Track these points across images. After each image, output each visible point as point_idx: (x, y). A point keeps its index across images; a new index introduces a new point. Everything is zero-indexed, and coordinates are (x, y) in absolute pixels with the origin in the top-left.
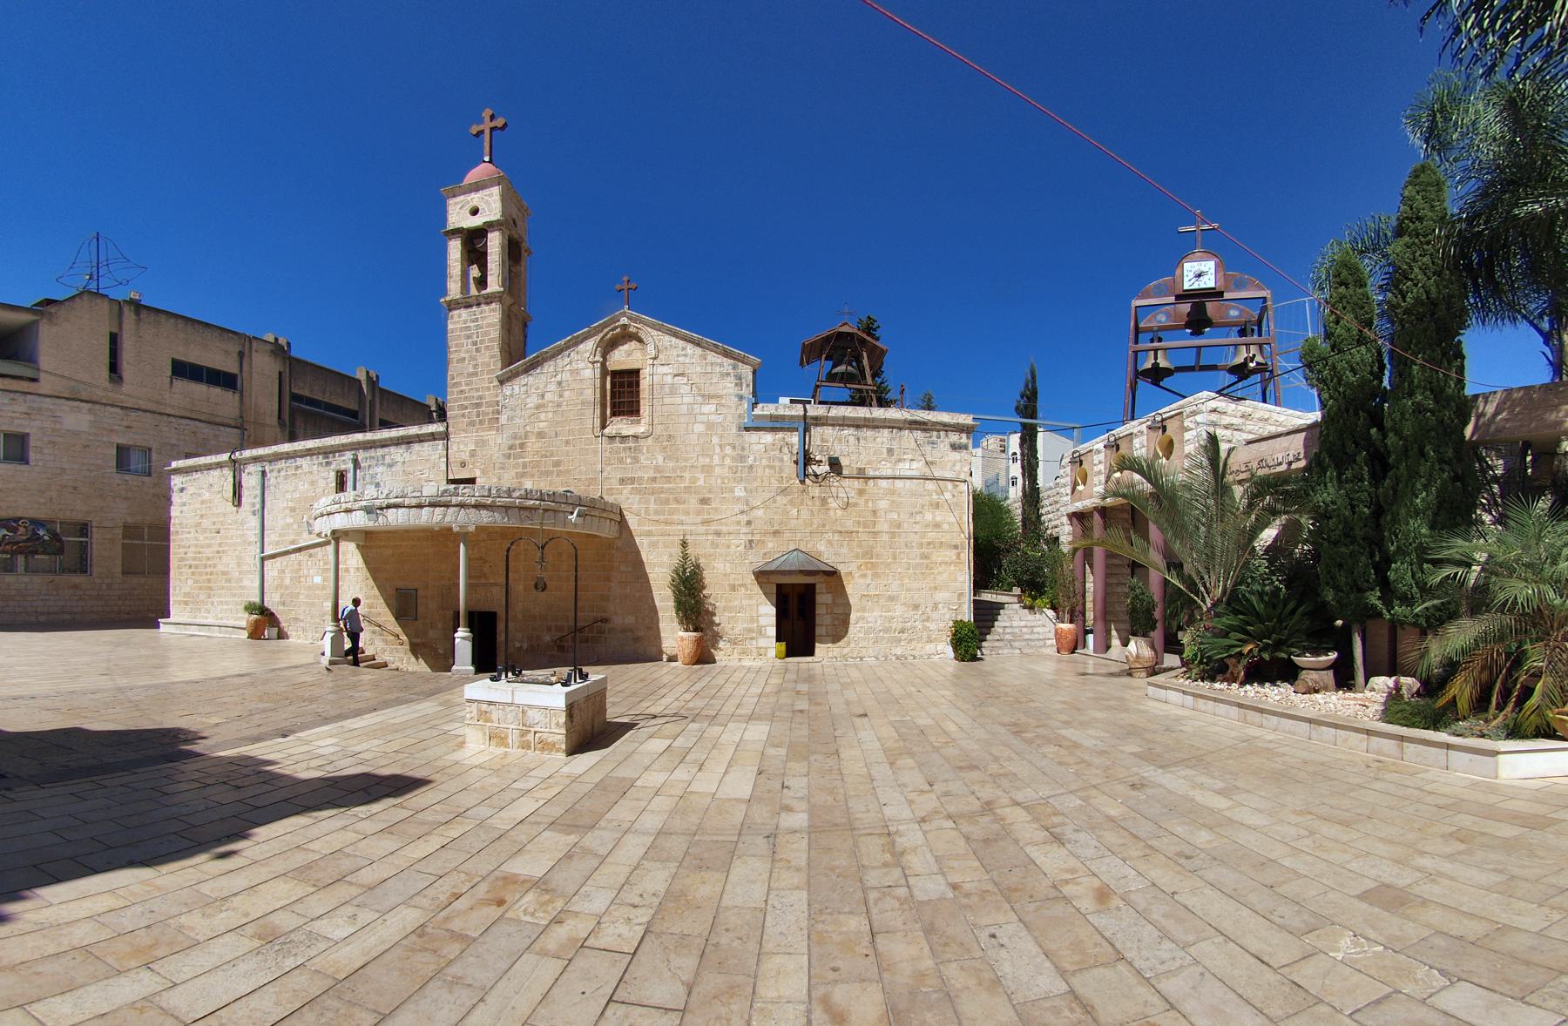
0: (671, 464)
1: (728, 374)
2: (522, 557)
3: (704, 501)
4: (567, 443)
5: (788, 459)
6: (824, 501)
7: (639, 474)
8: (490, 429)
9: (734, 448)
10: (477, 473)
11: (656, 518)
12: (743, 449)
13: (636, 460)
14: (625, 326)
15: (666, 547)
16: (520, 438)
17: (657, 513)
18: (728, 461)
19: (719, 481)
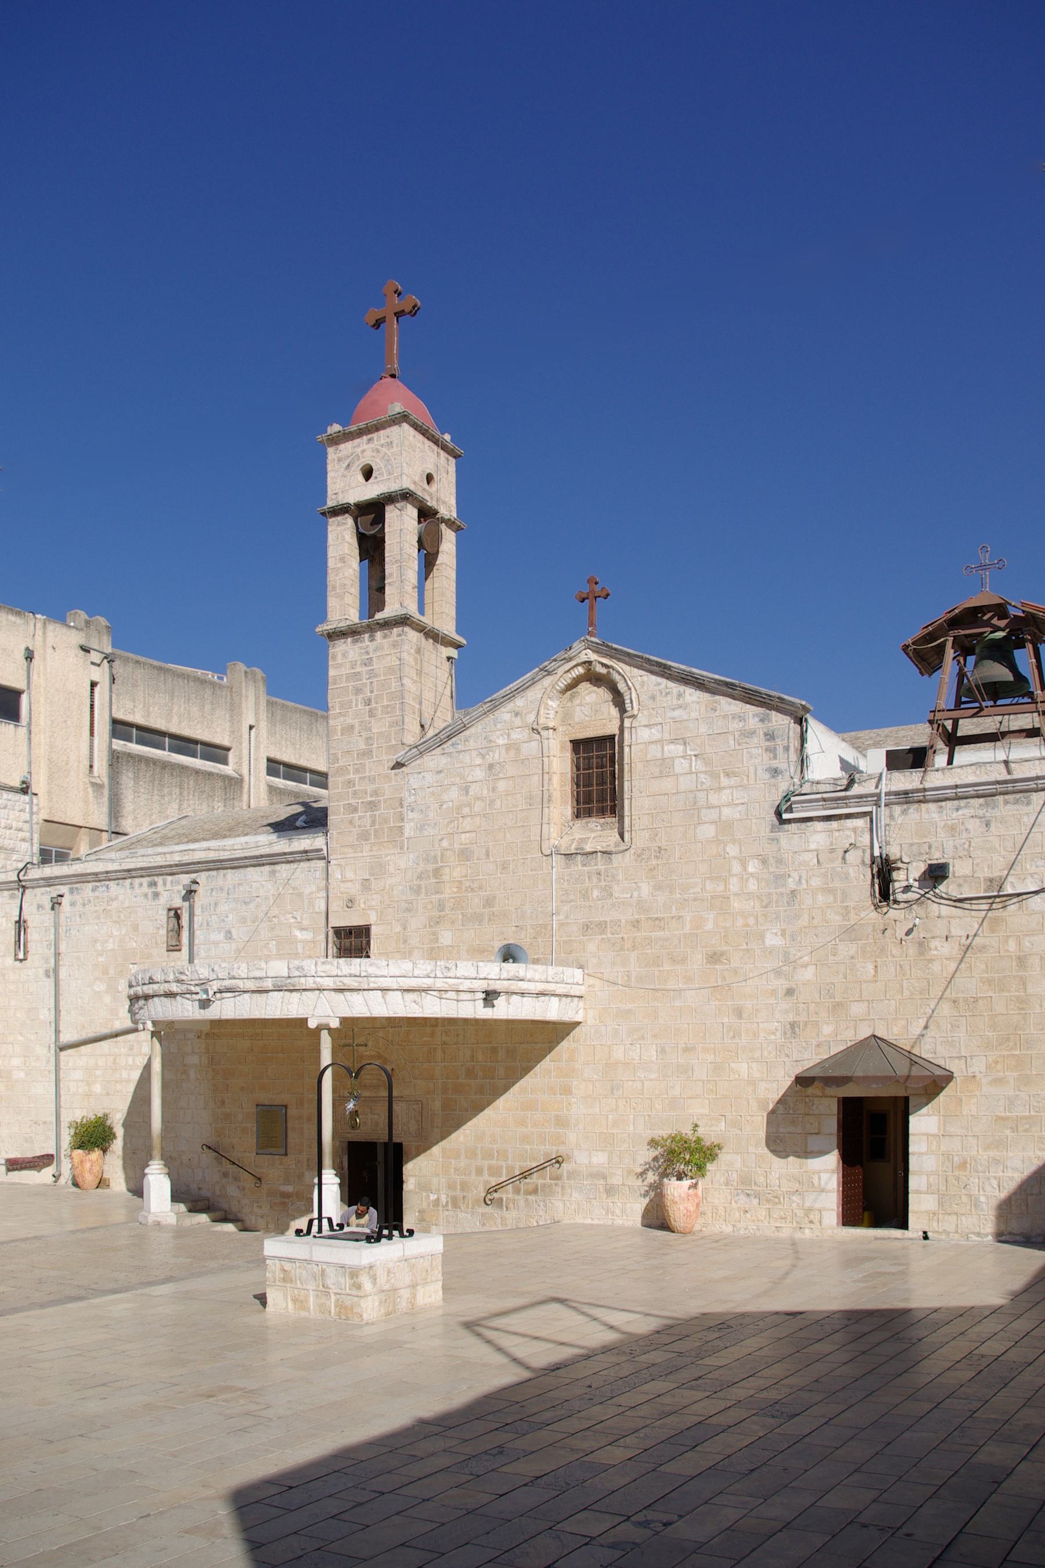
1: (752, 733)
2: (439, 1055)
3: (714, 958)
9: (764, 862)
12: (780, 861)
13: (608, 892)
18: (752, 886)
19: (740, 922)
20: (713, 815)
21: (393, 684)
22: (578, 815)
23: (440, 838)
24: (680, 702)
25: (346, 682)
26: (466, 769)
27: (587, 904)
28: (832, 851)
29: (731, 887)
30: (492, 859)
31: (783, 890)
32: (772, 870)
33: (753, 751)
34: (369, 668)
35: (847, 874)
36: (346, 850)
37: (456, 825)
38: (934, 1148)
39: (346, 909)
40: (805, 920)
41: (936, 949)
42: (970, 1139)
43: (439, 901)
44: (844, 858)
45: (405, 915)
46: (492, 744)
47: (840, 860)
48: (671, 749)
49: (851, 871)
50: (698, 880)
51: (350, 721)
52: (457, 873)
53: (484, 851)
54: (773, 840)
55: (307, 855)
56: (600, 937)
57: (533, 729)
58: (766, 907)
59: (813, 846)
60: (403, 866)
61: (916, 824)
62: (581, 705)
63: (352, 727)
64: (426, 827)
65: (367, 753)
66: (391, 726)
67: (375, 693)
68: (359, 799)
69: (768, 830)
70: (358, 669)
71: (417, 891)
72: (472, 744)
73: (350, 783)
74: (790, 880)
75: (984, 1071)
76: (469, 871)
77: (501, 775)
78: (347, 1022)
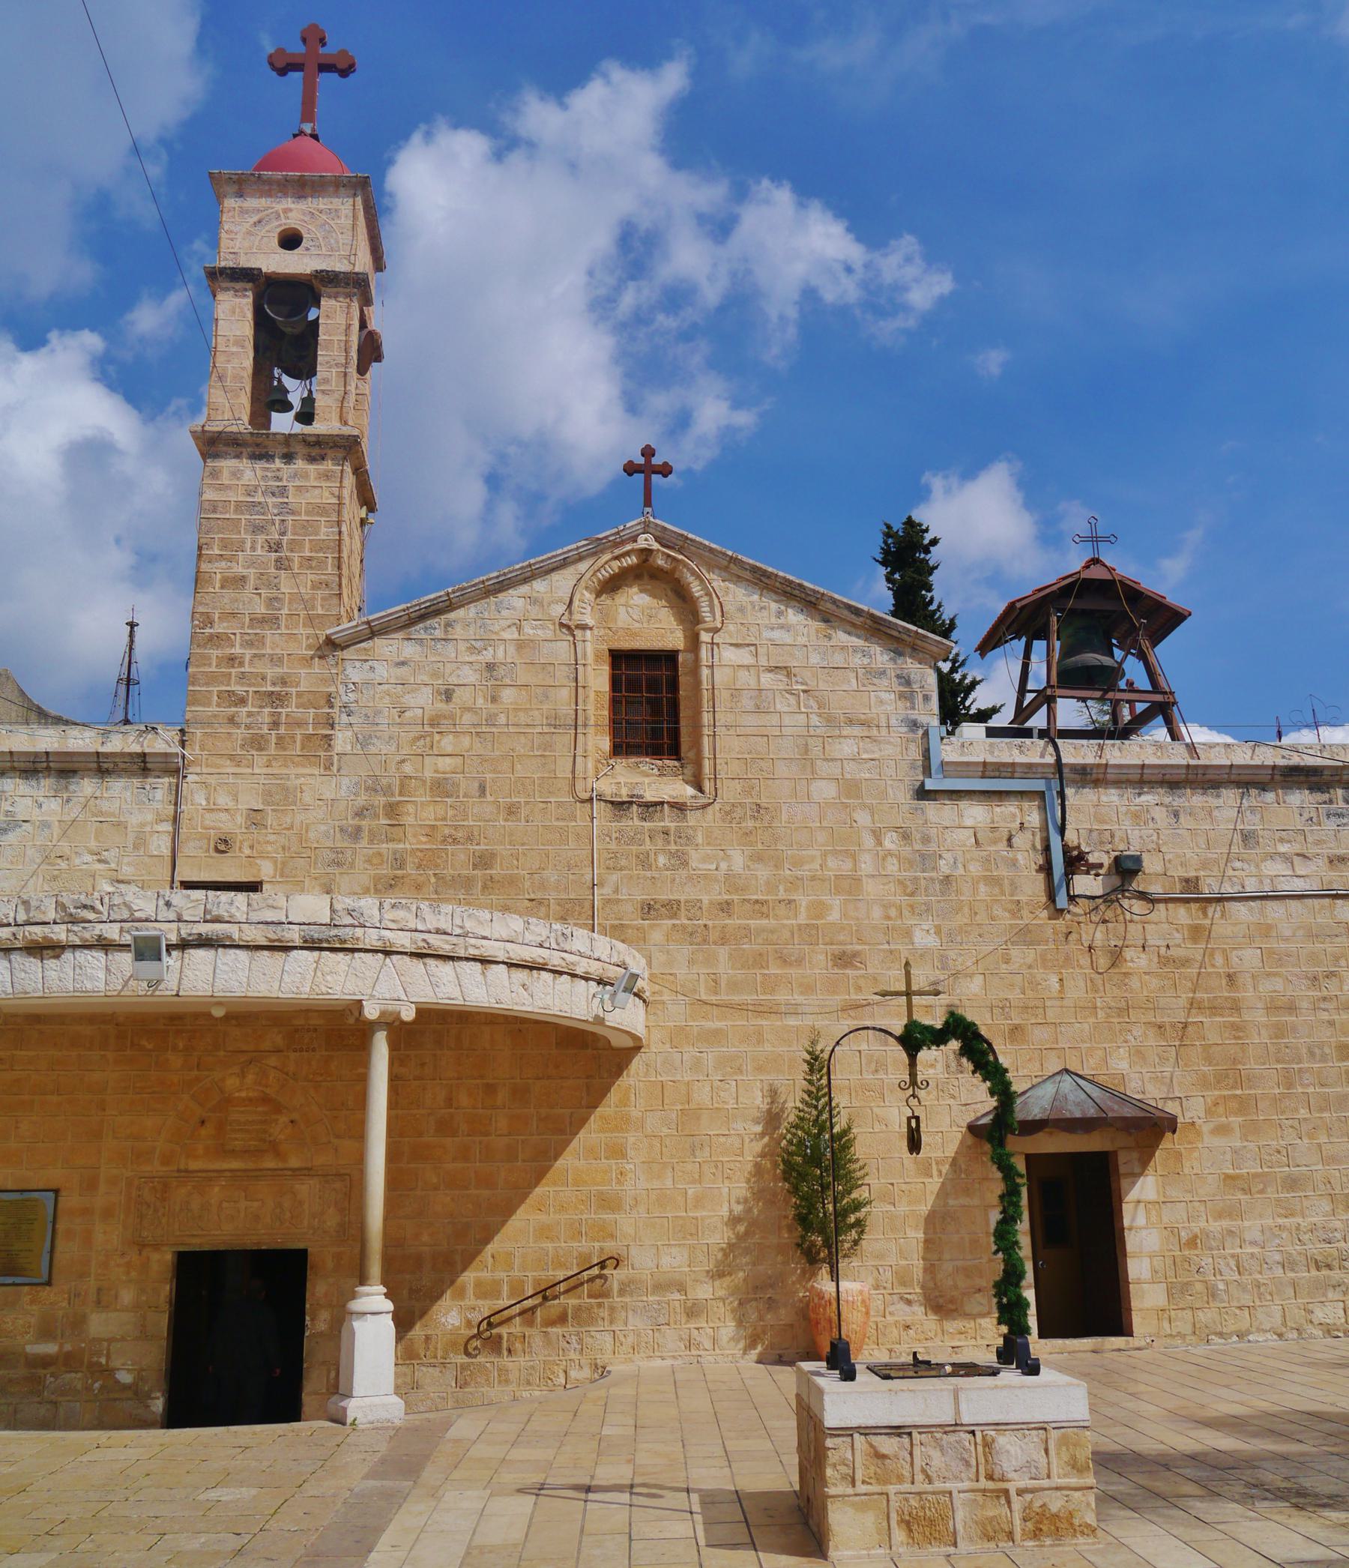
0: (763, 873)
3: (844, 960)
4: (512, 811)
5: (1028, 860)
6: (1116, 956)
7: (684, 894)
8: (308, 758)
9: (906, 837)
10: (265, 871)
11: (736, 998)
12: (926, 840)
13: (681, 860)
14: (647, 552)
15: (759, 1069)
16: (387, 791)
17: (734, 986)
18: (892, 866)
19: (877, 913)
20: (834, 769)
21: (324, 530)
22: (619, 749)
23: (398, 758)
24: (780, 621)
25: (236, 511)
26: (448, 665)
27: (648, 874)
28: (994, 829)
29: (863, 866)
30: (489, 798)
31: (934, 874)
32: (917, 847)
33: (884, 696)
34: (281, 500)
35: (1017, 860)
36: (219, 761)
37: (428, 744)
38: (1154, 1219)
39: (213, 853)
40: (961, 919)
41: (1133, 961)
42: (1197, 1204)
43: (395, 854)
44: (1009, 840)
45: (329, 870)
46: (494, 637)
47: (1005, 843)
48: (767, 679)
49: (1019, 856)
50: (814, 853)
51: (239, 569)
52: (429, 815)
53: (476, 785)
54: (916, 809)
55: (142, 765)
56: (671, 922)
57: (562, 625)
58: (912, 894)
59: (969, 822)
60: (328, 795)
61: (1094, 806)
62: (626, 606)
63: (243, 579)
64: (375, 741)
65: (272, 621)
66: (313, 588)
67: (289, 536)
68: (250, 685)
69: (908, 797)
70: (260, 499)
72: (458, 632)
73: (232, 660)
74: (942, 862)
75: (1202, 1115)
76: (450, 813)
77: (508, 681)
78: (427, 1014)
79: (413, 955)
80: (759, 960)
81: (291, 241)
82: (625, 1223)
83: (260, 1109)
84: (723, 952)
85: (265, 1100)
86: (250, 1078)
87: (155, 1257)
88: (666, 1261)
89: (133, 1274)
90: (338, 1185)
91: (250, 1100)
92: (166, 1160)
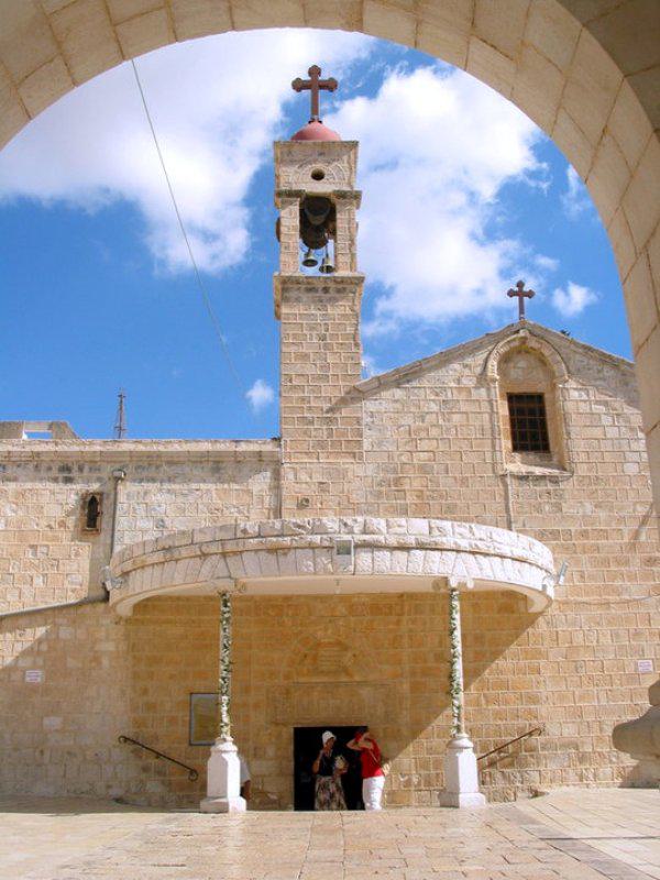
0: (602, 514)
15: (609, 623)
52: (417, 484)
71: (379, 495)
79: (470, 552)
80: (606, 562)
81: (318, 176)
82: (543, 709)
83: (335, 649)
84: (584, 558)
85: (339, 643)
86: (330, 631)
87: (285, 729)
88: (566, 732)
89: (273, 740)
90: (382, 690)
91: (330, 643)
92: (287, 677)
